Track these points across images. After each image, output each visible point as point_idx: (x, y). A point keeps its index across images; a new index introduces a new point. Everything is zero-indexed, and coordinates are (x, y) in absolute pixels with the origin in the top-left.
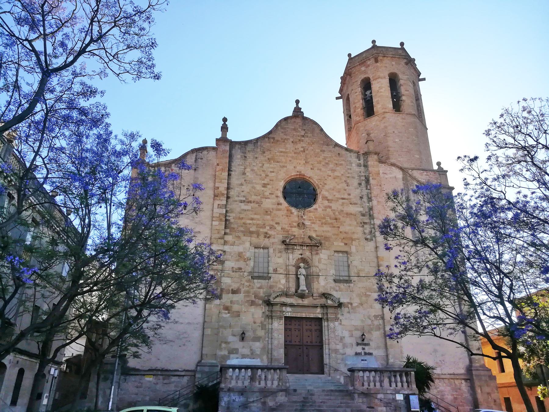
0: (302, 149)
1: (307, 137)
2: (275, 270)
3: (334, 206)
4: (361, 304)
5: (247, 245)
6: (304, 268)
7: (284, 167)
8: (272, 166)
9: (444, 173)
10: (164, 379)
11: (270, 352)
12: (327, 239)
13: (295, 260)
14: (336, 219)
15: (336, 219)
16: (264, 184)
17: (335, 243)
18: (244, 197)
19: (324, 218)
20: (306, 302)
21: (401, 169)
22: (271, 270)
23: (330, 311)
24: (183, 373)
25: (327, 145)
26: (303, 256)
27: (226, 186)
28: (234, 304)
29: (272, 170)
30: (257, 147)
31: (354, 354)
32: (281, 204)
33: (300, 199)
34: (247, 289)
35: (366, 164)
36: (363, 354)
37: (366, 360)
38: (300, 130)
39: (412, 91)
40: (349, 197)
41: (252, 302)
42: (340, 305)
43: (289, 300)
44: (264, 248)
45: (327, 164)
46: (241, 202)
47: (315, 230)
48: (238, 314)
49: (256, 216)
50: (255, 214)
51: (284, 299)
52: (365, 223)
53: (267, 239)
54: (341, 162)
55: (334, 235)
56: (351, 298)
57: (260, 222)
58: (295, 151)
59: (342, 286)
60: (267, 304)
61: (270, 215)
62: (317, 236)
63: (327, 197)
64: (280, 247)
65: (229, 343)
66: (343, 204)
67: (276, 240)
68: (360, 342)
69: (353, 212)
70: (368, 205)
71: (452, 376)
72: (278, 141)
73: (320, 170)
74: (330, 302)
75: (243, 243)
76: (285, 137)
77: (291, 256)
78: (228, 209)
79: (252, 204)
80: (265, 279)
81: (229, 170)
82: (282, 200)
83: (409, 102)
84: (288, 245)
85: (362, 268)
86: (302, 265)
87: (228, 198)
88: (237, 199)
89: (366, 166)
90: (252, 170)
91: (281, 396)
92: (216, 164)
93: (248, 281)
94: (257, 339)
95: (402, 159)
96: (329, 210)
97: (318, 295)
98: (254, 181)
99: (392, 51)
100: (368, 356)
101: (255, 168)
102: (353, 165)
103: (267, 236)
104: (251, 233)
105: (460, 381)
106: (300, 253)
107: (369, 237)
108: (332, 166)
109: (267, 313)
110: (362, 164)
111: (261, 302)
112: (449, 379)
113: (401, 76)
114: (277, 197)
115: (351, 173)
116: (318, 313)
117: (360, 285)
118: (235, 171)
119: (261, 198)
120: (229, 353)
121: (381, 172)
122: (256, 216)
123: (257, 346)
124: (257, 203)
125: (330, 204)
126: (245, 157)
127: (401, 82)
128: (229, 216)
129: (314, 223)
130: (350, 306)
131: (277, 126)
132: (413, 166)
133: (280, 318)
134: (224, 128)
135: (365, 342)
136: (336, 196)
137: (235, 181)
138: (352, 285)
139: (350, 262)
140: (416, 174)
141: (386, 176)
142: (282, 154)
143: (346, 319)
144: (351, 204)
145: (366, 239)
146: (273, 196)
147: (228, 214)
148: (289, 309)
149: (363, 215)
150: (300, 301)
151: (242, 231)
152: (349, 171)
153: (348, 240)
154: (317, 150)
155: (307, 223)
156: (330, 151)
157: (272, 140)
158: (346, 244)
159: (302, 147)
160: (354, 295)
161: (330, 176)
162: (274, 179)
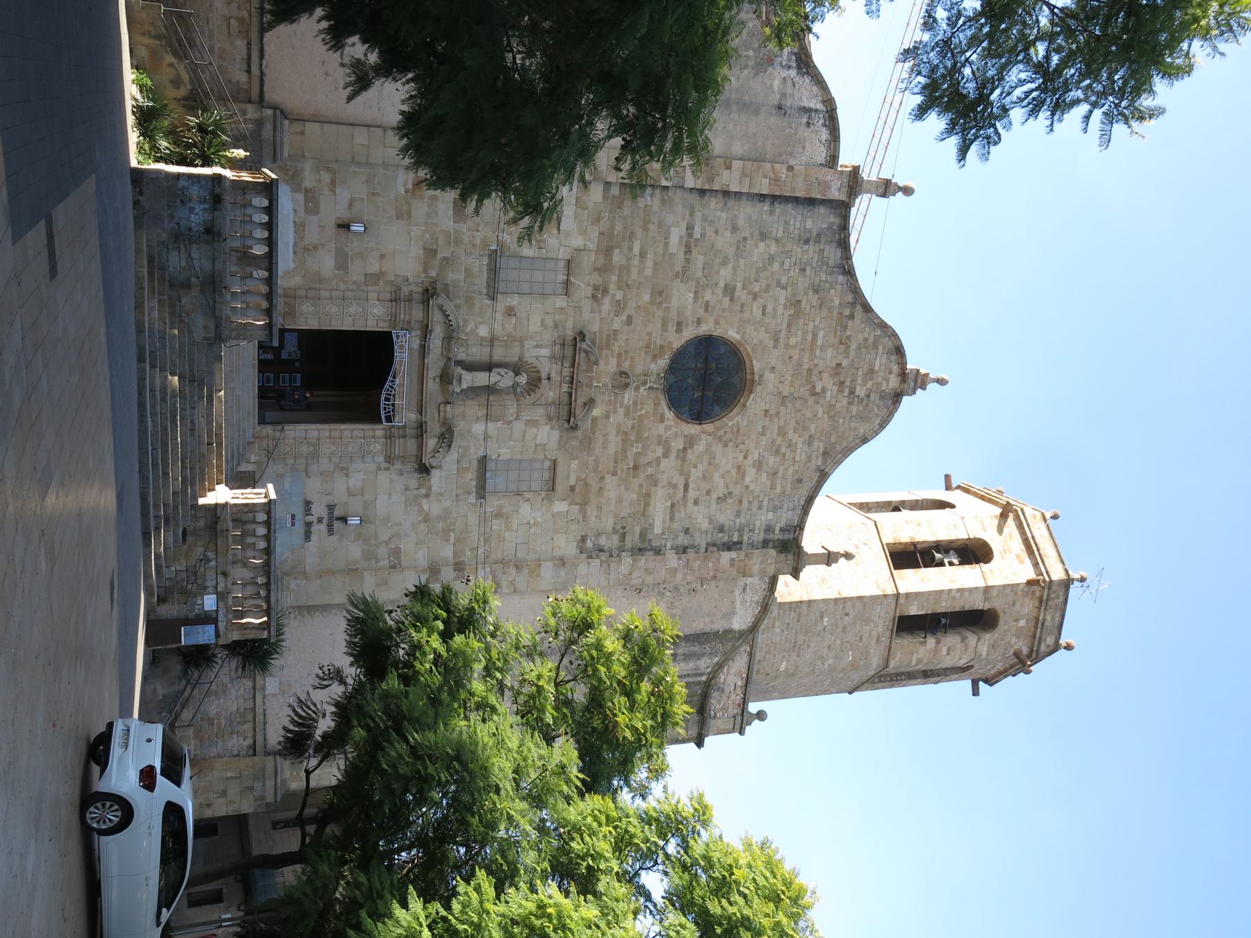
0: (818, 389)
1: (850, 403)
2: (510, 312)
3: (669, 464)
4: (426, 519)
5: (578, 242)
6: (515, 386)
7: (776, 340)
8: (780, 310)
9: (737, 726)
10: (240, 20)
11: (311, 293)
12: (587, 444)
13: (533, 360)
14: (636, 468)
15: (636, 468)
16: (734, 288)
17: (574, 464)
18: (703, 235)
19: (638, 439)
20: (432, 386)
21: (754, 628)
22: (514, 301)
23: (411, 446)
24: (255, 70)
25: (825, 454)
26: (545, 382)
27: (734, 188)
28: (430, 205)
29: (770, 308)
30: (831, 274)
31: (308, 499)
32: (679, 331)
33: (690, 381)
34: (466, 239)
35: (771, 544)
36: (309, 519)
37: (293, 524)
38: (869, 385)
39: (947, 662)
40: (691, 501)
41: (433, 252)
42: (424, 470)
43: (436, 343)
44: (567, 283)
45: (777, 451)
46: (690, 228)
47: (610, 417)
48: (403, 215)
49: (649, 264)
50: (656, 264)
51: (438, 332)
52: (623, 536)
53: (589, 292)
54: (779, 489)
55: (597, 461)
56: (441, 494)
57: (634, 275)
58: (815, 372)
59: (471, 477)
60: (427, 290)
61: (652, 302)
62: (594, 420)
63: (692, 447)
64: (570, 325)
65: (333, 191)
66: (675, 486)
67: (587, 315)
68: (337, 513)
69: (651, 508)
70: (669, 545)
71: (259, 718)
72: (845, 327)
73: (763, 434)
74: (431, 443)
75: (583, 232)
76: (853, 346)
77: (545, 352)
78: (670, 193)
79: (681, 256)
80: (488, 286)
81: (774, 198)
82: (688, 334)
83: (921, 655)
84: (576, 348)
85: (515, 526)
86: (523, 379)
87: (702, 192)
88: (698, 215)
89: (765, 544)
90: (771, 259)
91: (205, 327)
92: (792, 162)
93: (485, 243)
94: (342, 263)
95: (778, 630)
96: (660, 451)
97: (449, 415)
98: (742, 262)
99: (1053, 619)
100: (302, 532)
101: (776, 266)
102: (770, 515)
103: (599, 292)
104: (608, 252)
105: (250, 734)
106: (553, 375)
107: (589, 544)
108: (771, 463)
109: (406, 290)
110: (771, 536)
111: (433, 274)
112: (254, 709)
113: (988, 637)
114: (699, 322)
115: (749, 509)
116: (406, 416)
117: (473, 518)
118: (772, 212)
119: (698, 280)
120: (307, 191)
121: (749, 580)
122: (649, 264)
123: (326, 263)
124: (685, 269)
125: (673, 456)
126: (807, 241)
127: (972, 639)
128: (652, 195)
129: (627, 414)
130: (423, 491)
131: (883, 326)
132: (758, 655)
133: (394, 321)
134: (886, 188)
135: (337, 525)
136: (693, 471)
137: (746, 212)
138: (472, 499)
139: (527, 495)
140: (739, 663)
141: (737, 592)
142: (810, 337)
143: (392, 481)
144: (673, 505)
145: (583, 539)
146: (701, 312)
147: (658, 192)
148: (416, 343)
149: (643, 535)
150: (433, 372)
151: (613, 227)
152: (756, 504)
153: (581, 495)
154: (813, 426)
155: (628, 396)
156: (809, 458)
157: (847, 312)
158: (572, 489)
159: (824, 390)
160: (447, 504)
161: (745, 457)
162: (747, 315)
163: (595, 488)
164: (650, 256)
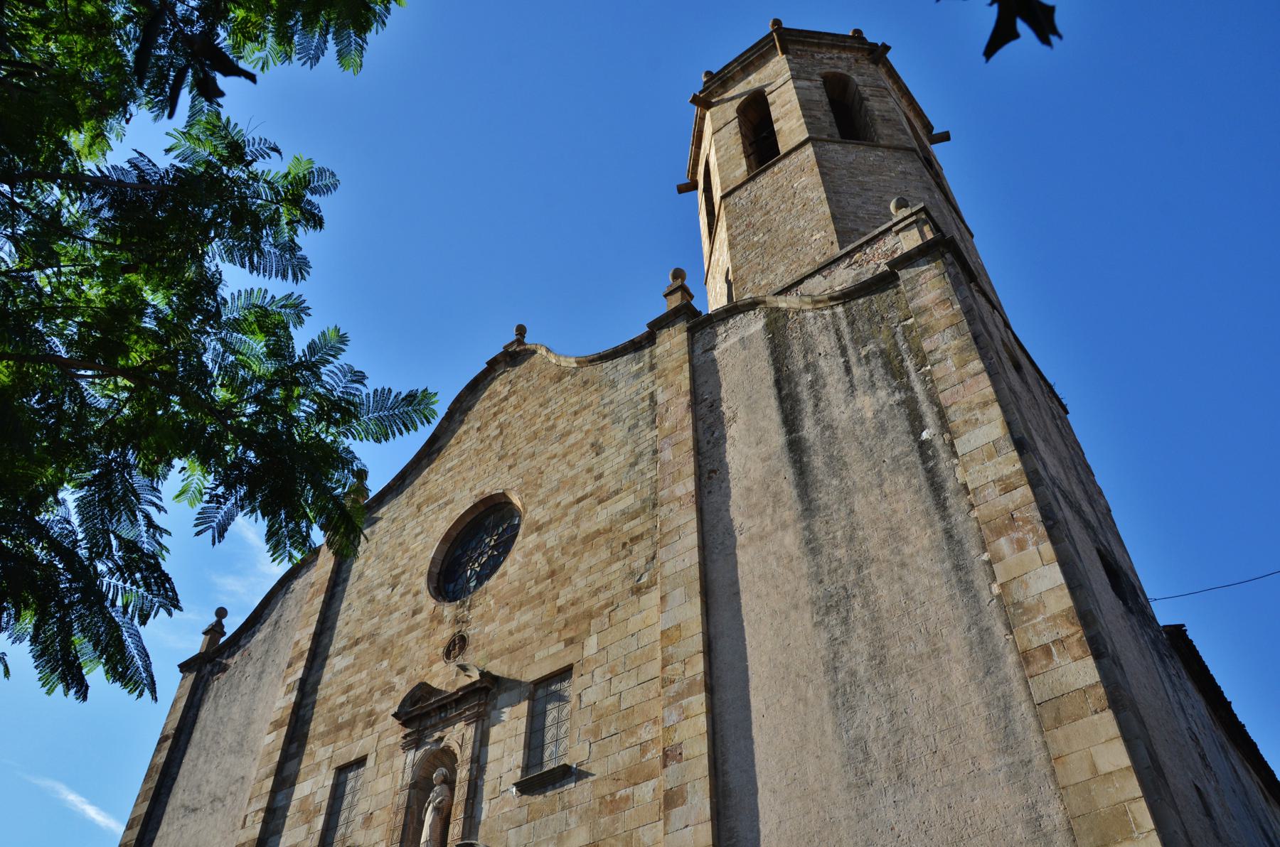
7: (446, 504)
69: (601, 526)
79: (356, 649)
119: (381, 618)
144: (600, 503)
146: (409, 597)
160: (573, 820)
163: (571, 612)
164: (352, 680)
